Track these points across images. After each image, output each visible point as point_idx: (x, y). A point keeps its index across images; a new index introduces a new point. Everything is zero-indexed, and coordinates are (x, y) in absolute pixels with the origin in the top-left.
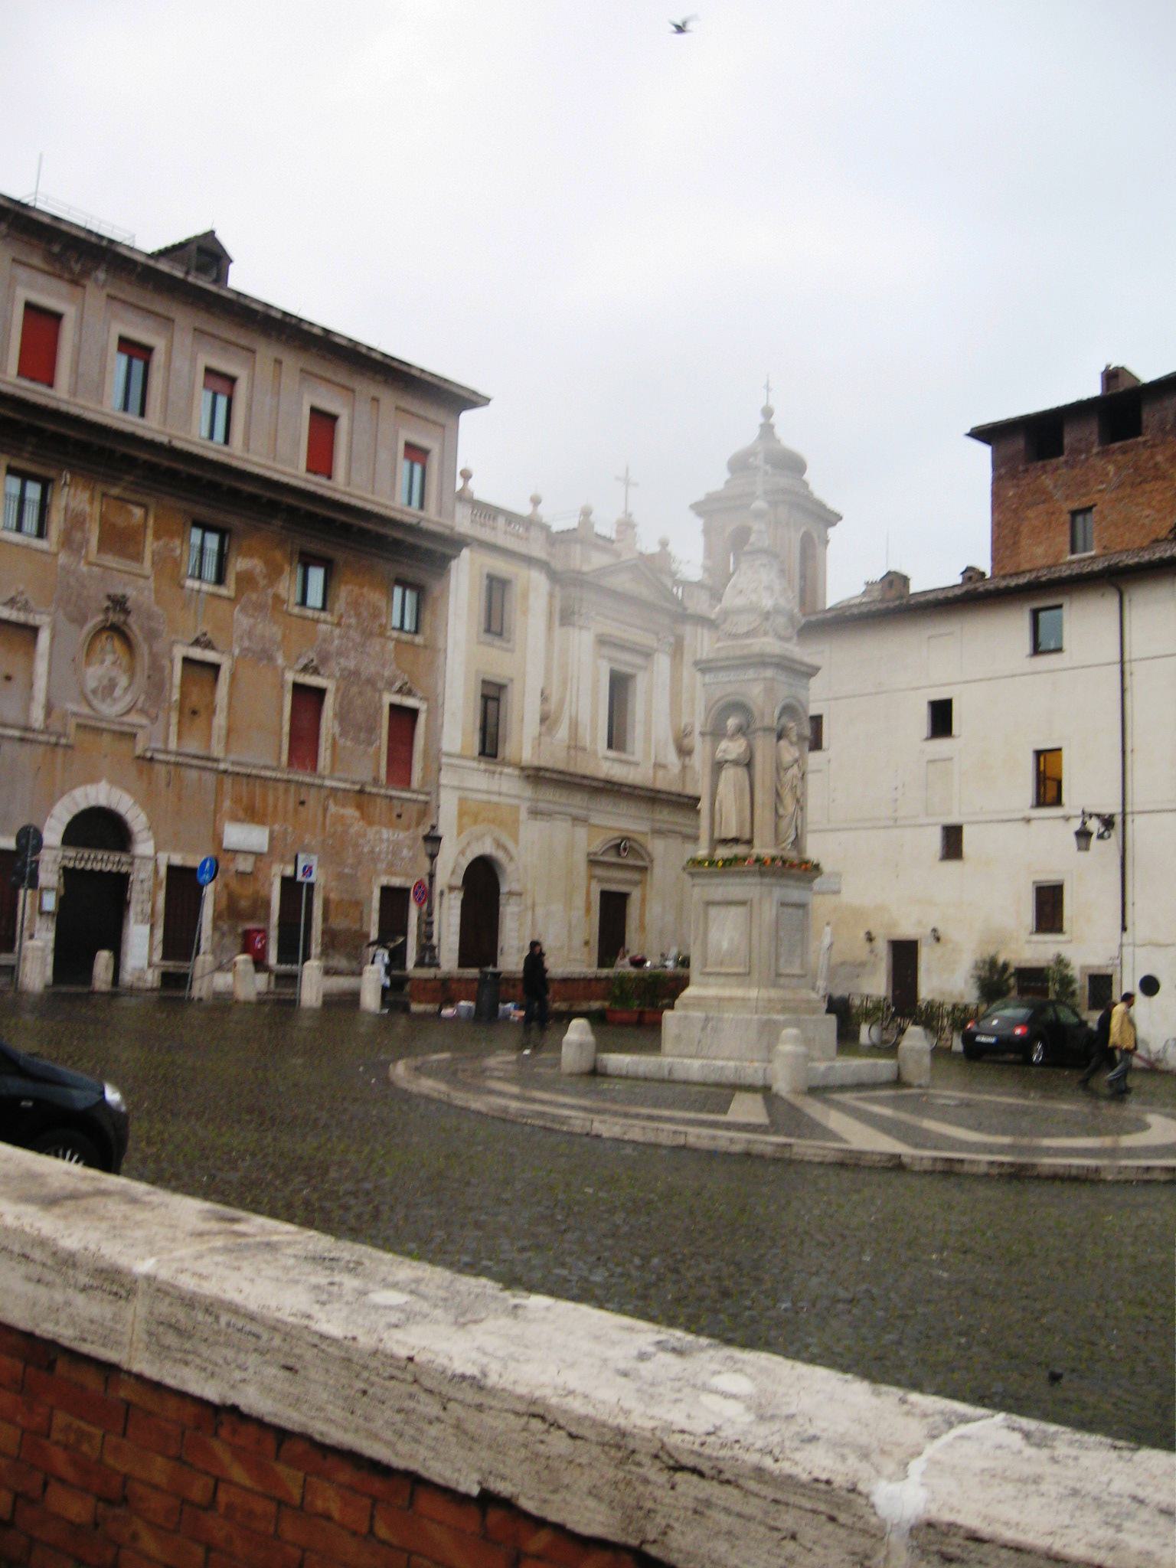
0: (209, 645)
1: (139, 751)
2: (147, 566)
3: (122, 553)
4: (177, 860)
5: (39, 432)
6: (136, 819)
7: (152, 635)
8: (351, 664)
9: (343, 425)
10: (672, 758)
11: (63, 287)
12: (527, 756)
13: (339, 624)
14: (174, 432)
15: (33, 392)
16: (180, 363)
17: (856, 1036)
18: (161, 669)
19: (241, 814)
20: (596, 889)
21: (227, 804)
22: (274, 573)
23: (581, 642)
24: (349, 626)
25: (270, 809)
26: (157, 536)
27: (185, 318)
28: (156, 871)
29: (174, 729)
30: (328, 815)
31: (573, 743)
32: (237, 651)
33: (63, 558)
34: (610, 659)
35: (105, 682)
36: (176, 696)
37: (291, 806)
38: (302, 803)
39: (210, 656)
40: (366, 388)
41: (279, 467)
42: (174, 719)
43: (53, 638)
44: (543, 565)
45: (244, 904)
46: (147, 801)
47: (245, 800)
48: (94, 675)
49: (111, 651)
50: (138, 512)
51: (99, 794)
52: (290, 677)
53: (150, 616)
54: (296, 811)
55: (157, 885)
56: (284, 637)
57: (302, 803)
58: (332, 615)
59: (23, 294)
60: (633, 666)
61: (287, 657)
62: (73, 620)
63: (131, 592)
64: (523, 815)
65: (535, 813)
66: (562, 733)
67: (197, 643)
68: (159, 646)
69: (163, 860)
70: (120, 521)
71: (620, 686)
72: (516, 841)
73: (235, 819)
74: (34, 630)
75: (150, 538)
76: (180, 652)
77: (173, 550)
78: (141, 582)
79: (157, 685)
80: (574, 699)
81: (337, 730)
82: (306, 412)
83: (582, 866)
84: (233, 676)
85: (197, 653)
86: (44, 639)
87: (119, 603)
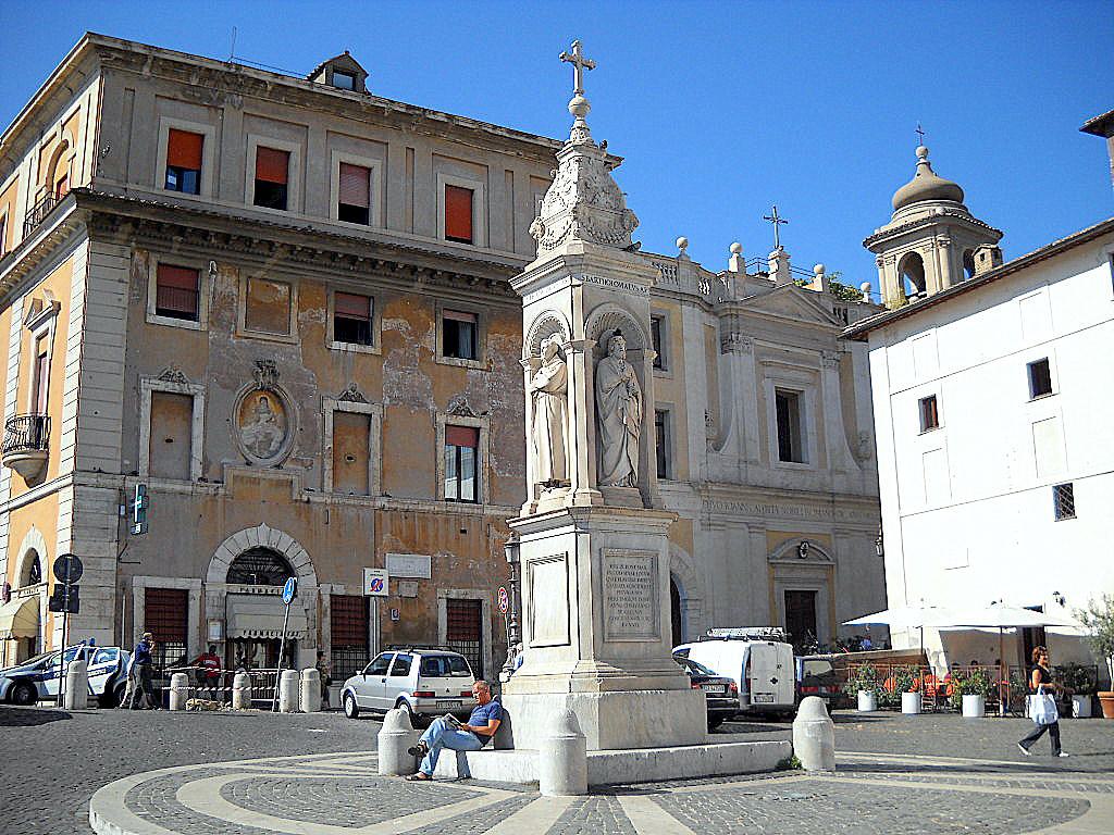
0: (360, 399)
1: (296, 496)
2: (294, 332)
3: (271, 327)
4: (340, 590)
5: (181, 231)
6: (297, 555)
7: (302, 393)
8: (505, 404)
9: (479, 196)
10: (850, 463)
11: (203, 112)
12: (695, 471)
13: (489, 370)
14: (311, 218)
15: (184, 198)
16: (316, 161)
17: (1070, 709)
18: (314, 423)
19: (402, 546)
20: (780, 590)
21: (387, 537)
22: (419, 330)
23: (741, 364)
24: (500, 370)
25: (431, 541)
26: (301, 308)
27: (317, 122)
28: (320, 600)
29: (328, 473)
30: (491, 541)
31: (743, 458)
32: (387, 402)
33: (212, 335)
34: (774, 379)
35: (261, 438)
36: (329, 445)
37: (452, 536)
38: (464, 532)
39: (360, 407)
40: (499, 161)
41: (417, 238)
42: (328, 466)
43: (206, 404)
44: (695, 299)
45: (410, 625)
46: (305, 540)
47: (404, 535)
48: (249, 432)
49: (265, 408)
50: (283, 289)
51: (260, 536)
52: (442, 420)
53: (300, 377)
54: (457, 539)
55: (322, 613)
56: (434, 384)
57: (464, 532)
58: (481, 362)
59: (167, 122)
60: (795, 381)
61: (436, 403)
62: (225, 387)
63: (279, 359)
64: (697, 527)
65: (708, 525)
66: (730, 448)
67: (346, 397)
68: (312, 403)
69: (326, 589)
70: (267, 299)
71: (787, 405)
72: (690, 551)
73: (397, 551)
74: (191, 397)
75: (295, 310)
76: (330, 406)
77: (319, 319)
78: (289, 349)
79: (312, 436)
80: (740, 417)
81: (494, 465)
82: (442, 189)
83: (764, 567)
84: (384, 423)
85: (347, 406)
86: (199, 403)
87: (266, 367)
